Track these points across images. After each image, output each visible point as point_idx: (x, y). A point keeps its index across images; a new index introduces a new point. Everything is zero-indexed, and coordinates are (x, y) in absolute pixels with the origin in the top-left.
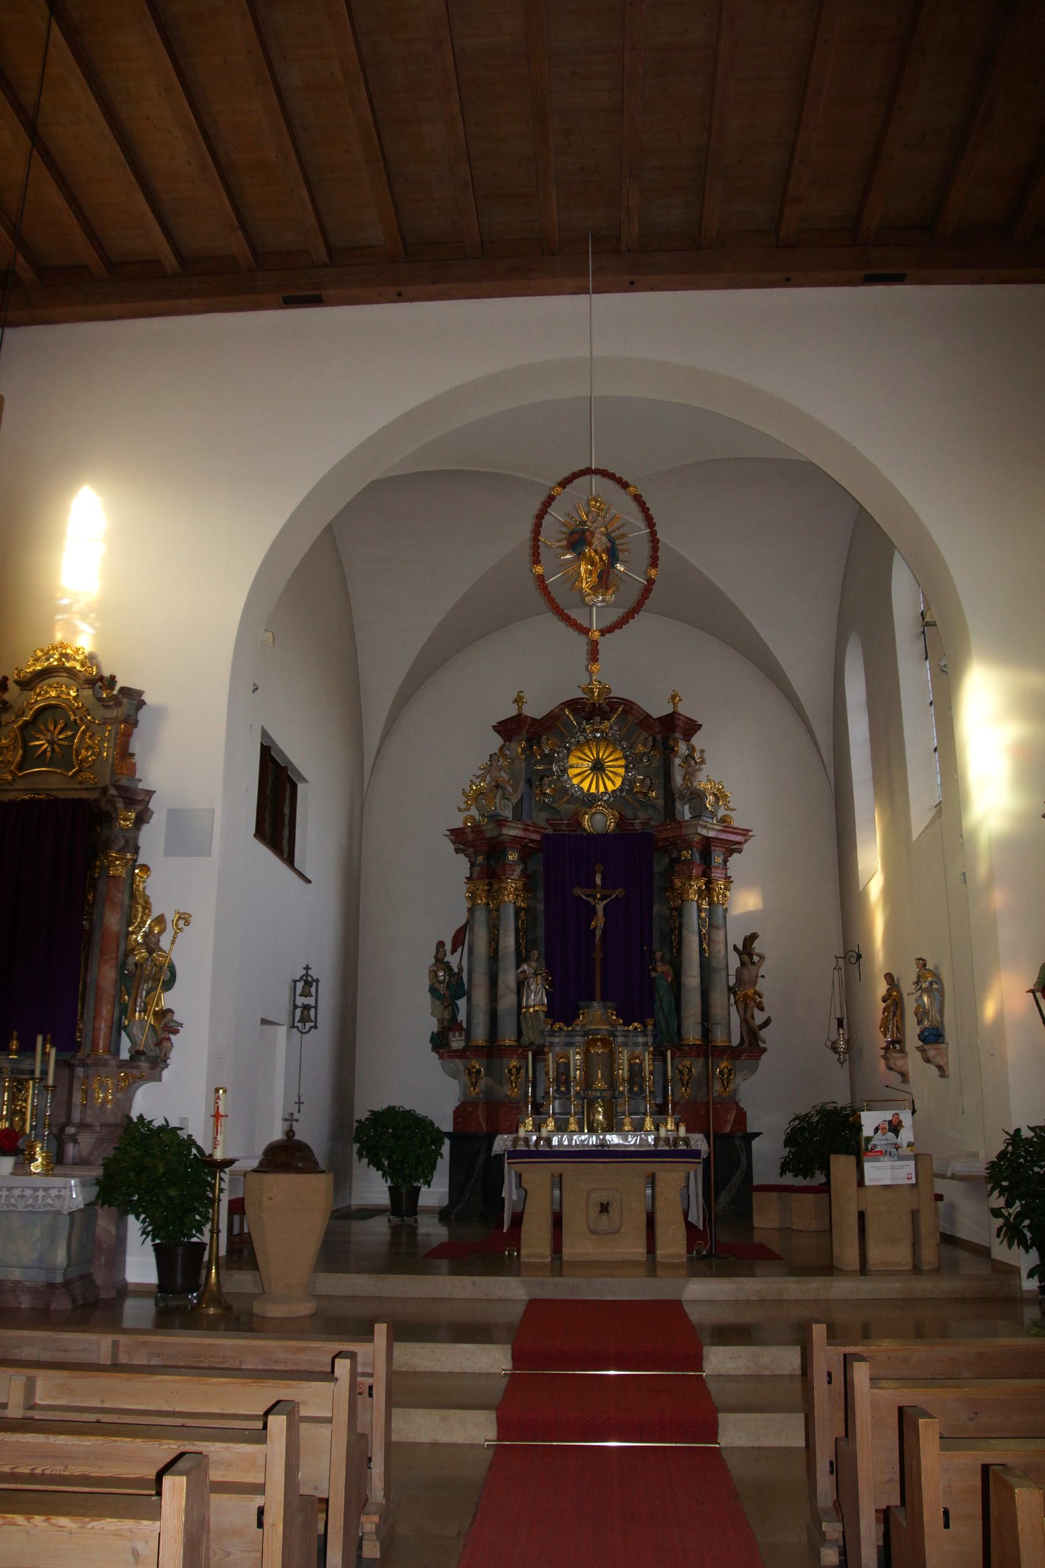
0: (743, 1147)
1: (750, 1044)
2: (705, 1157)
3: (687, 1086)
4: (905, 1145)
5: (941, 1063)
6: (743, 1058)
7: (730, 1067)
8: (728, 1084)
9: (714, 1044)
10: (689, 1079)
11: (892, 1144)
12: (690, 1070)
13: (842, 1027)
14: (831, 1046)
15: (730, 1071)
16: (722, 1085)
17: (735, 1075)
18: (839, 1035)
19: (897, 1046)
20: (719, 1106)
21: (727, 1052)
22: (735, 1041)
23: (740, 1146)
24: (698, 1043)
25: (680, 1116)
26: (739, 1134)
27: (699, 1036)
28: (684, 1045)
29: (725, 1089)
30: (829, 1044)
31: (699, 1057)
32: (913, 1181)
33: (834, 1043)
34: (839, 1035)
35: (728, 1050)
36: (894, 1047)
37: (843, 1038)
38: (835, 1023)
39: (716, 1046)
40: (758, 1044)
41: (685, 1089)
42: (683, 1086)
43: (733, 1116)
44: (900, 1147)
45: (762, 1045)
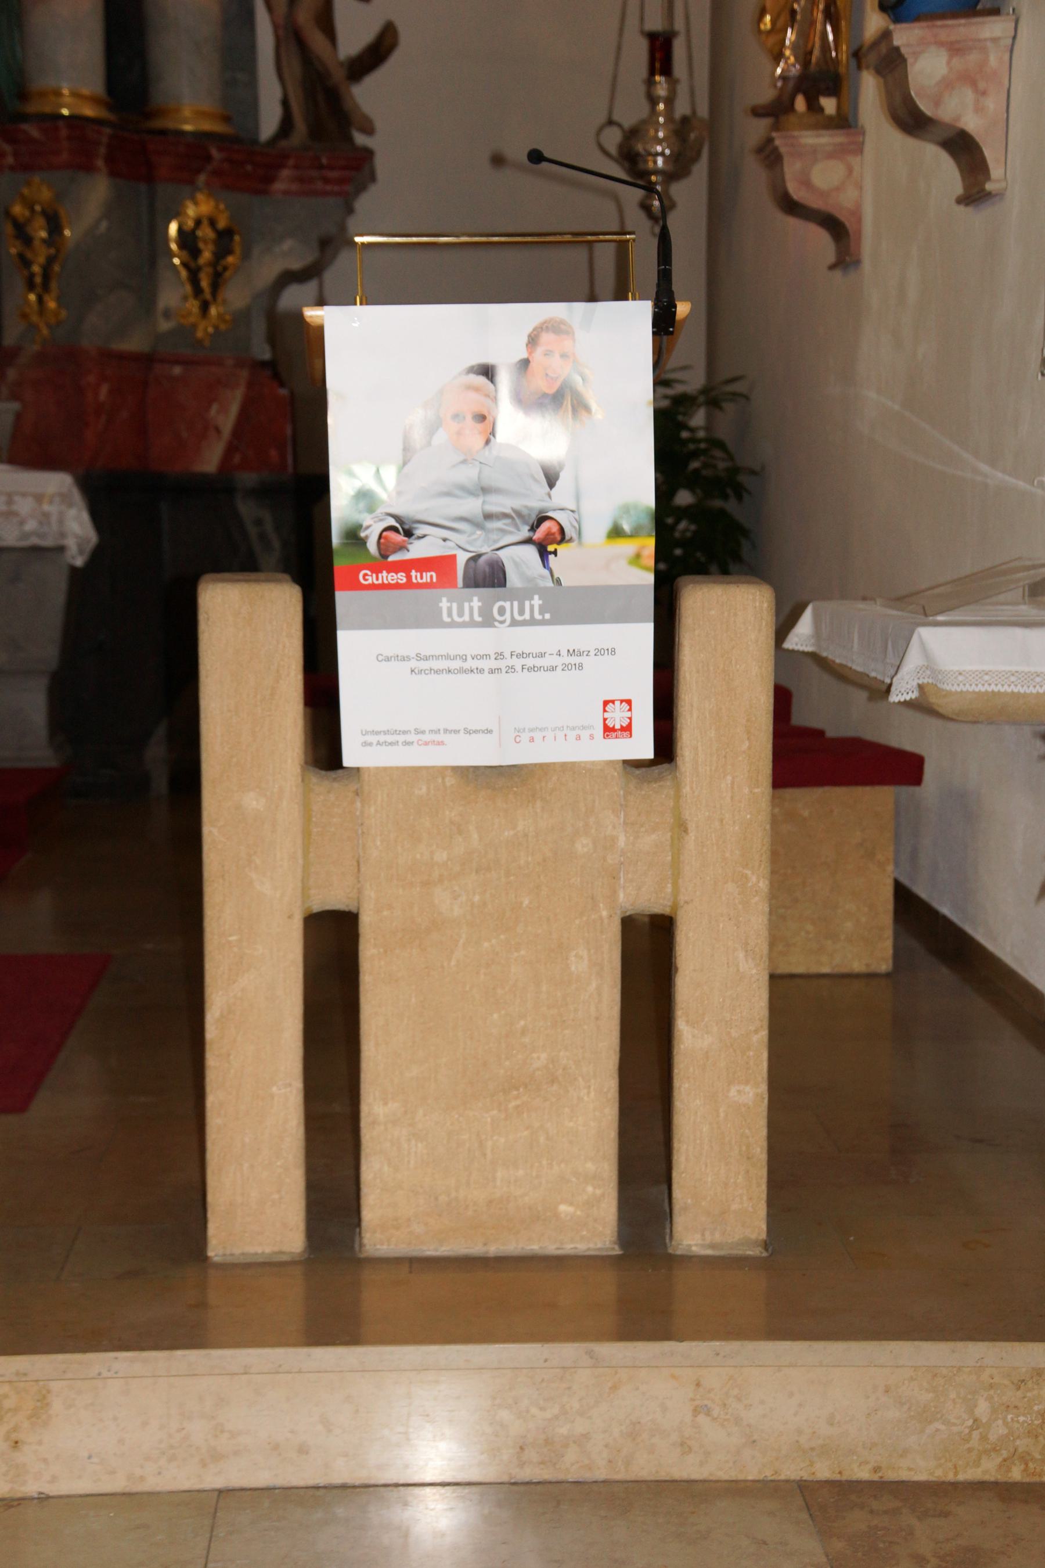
0: (269, 526)
1: (316, 132)
2: (79, 562)
3: (46, 286)
4: (595, 530)
5: (971, 124)
6: (279, 186)
7: (222, 224)
8: (215, 286)
9: (159, 124)
10: (51, 260)
11: (516, 516)
12: (54, 225)
13: (667, 70)
14: (621, 147)
15: (224, 238)
16: (188, 288)
17: (246, 255)
18: (653, 101)
19: (829, 105)
20: (177, 370)
21: (209, 158)
22: (269, 123)
23: (259, 522)
24: (89, 111)
25: (15, 406)
26: (248, 479)
27: (94, 83)
28: (25, 118)
29: (205, 307)
30: (613, 139)
31: (88, 168)
32: (643, 746)
33: (633, 134)
34: (653, 101)
35: (215, 153)
36: (814, 106)
37: (669, 118)
38: (638, 52)
39: (163, 132)
40: (350, 139)
41: (40, 299)
42: (31, 286)
43: (234, 409)
44: (562, 537)
45: (360, 139)
